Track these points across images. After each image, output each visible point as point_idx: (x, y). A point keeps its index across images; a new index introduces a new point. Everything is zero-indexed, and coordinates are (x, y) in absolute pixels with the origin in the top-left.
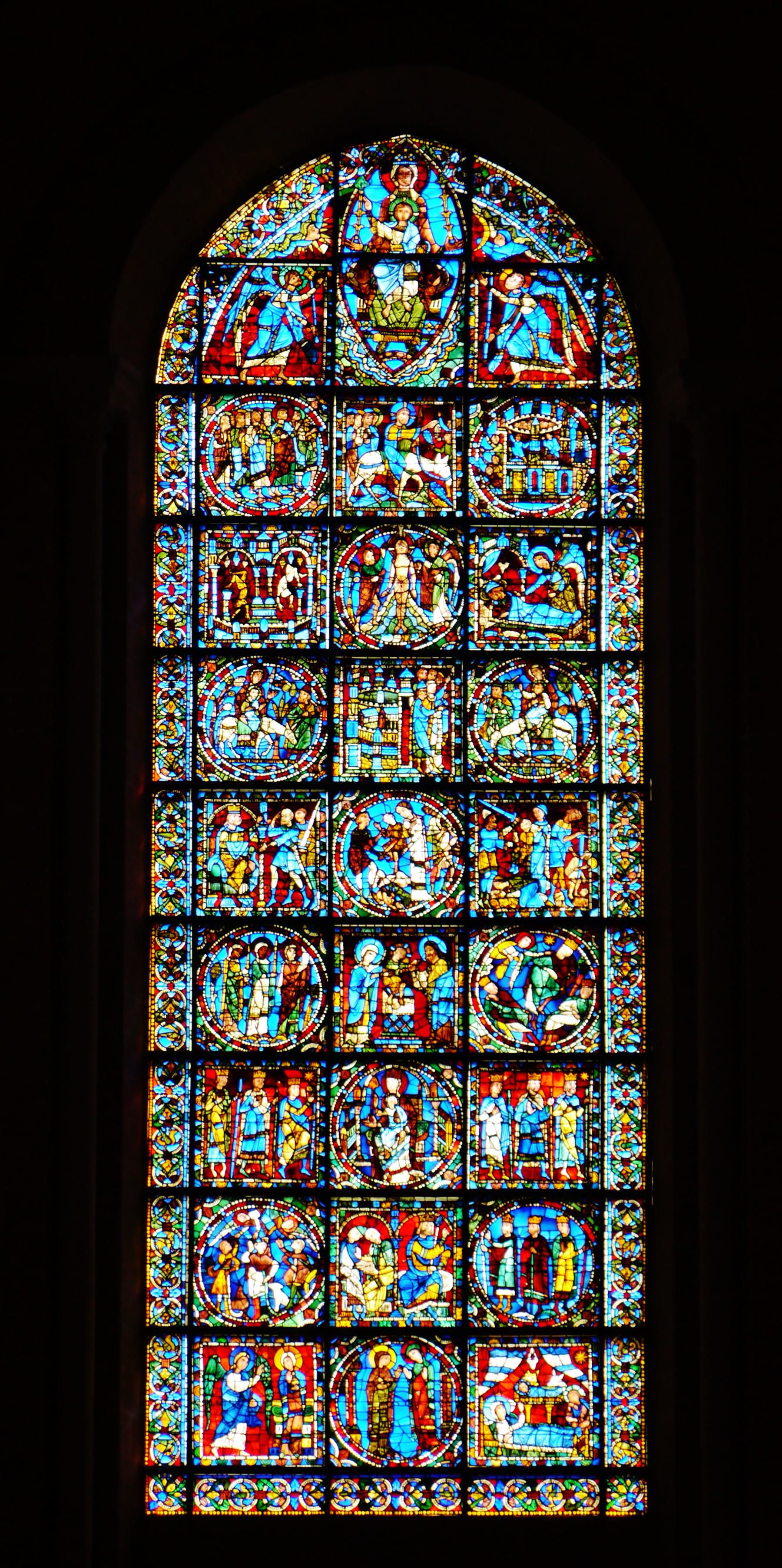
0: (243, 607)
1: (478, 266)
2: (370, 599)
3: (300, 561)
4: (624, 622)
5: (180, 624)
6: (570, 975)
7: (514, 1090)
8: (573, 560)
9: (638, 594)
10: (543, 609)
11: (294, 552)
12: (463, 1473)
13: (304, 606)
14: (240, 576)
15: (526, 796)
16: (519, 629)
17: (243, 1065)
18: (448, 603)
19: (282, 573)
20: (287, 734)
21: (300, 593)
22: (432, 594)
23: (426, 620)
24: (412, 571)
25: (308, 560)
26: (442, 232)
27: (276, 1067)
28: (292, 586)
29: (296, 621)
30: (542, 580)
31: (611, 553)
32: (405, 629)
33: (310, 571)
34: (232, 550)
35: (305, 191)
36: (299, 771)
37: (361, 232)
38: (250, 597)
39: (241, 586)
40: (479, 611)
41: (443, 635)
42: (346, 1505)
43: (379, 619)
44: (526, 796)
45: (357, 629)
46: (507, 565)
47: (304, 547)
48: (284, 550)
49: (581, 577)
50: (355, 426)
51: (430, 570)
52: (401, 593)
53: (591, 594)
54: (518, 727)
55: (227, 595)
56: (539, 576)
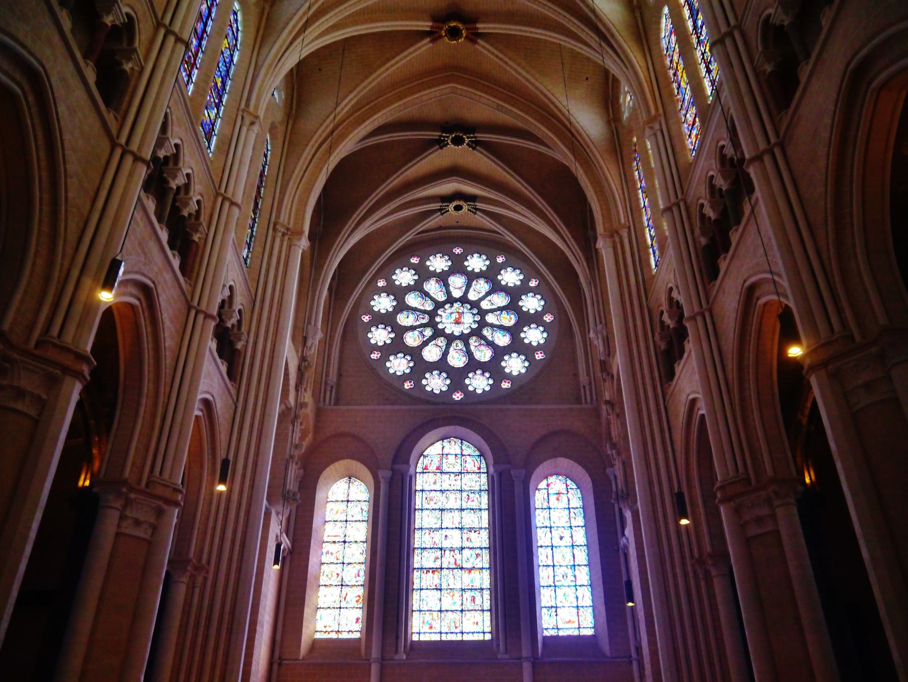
1: (463, 455)
6: (478, 555)
7: (470, 572)
8: (477, 495)
12: (462, 633)
15: (470, 530)
17: (428, 570)
20: (436, 521)
26: (459, 452)
27: (434, 570)
35: (438, 445)
36: (438, 526)
37: (446, 451)
42: (444, 638)
44: (470, 530)
50: (446, 477)
54: (470, 519)
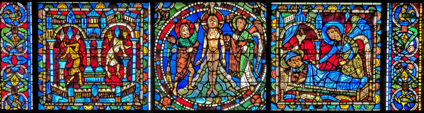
0: (76, 75)
2: (186, 67)
3: (125, 35)
4: (405, 86)
5: (22, 90)
9: (417, 62)
10: (334, 75)
11: (119, 27)
13: (129, 74)
14: (73, 48)
16: (314, 93)
18: (253, 71)
19: (111, 45)
21: (125, 63)
22: (239, 62)
23: (234, 84)
24: (222, 42)
25: (132, 33)
28: (118, 56)
29: (122, 86)
30: (334, 50)
31: (394, 25)
32: (216, 93)
33: (134, 43)
34: (66, 25)
38: (82, 66)
39: (74, 56)
40: (279, 76)
41: (249, 97)
43: (193, 84)
45: (175, 93)
46: (304, 37)
47: (129, 23)
48: (111, 26)
49: (367, 47)
51: (237, 42)
52: (213, 62)
53: (378, 62)
55: (63, 65)
56: (332, 46)
